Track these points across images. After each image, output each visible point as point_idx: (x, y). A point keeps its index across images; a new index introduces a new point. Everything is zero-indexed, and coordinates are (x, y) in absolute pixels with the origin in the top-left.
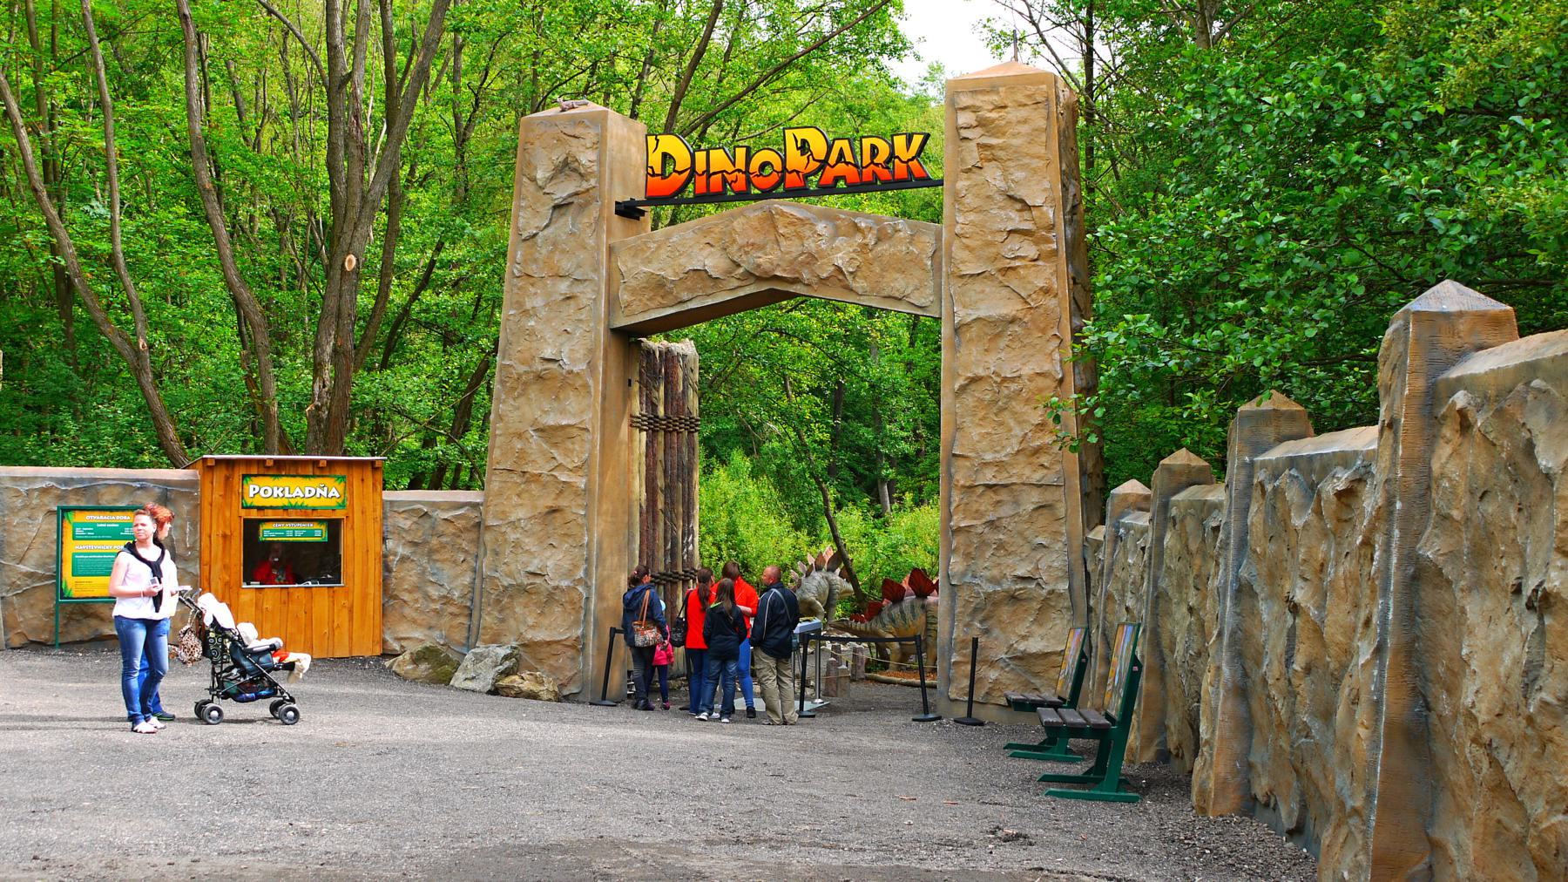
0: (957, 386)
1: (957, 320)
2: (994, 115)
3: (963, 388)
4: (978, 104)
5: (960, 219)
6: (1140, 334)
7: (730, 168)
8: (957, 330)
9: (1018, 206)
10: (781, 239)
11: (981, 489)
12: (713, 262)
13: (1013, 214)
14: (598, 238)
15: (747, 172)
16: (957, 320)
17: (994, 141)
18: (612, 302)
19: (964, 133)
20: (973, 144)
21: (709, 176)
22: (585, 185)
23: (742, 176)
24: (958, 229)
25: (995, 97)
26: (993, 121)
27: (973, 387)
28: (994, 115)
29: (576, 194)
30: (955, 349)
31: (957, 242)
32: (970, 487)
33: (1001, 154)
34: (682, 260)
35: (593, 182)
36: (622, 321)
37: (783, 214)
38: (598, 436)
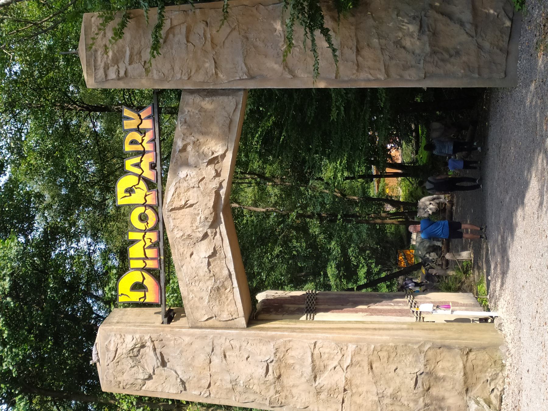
0: (290, 76)
1: (245, 77)
2: (110, 54)
3: (291, 72)
4: (102, 65)
5: (179, 76)
6: (59, 169)
7: (142, 243)
8: (252, 78)
9: (171, 36)
10: (190, 203)
11: (360, 59)
12: (204, 250)
13: (176, 39)
14: (185, 334)
15: (145, 231)
16: (245, 77)
17: (128, 53)
18: (228, 325)
19: (122, 74)
20: (129, 68)
21: (147, 258)
22: (149, 344)
23: (148, 235)
24: (185, 78)
25: (99, 53)
26: (114, 54)
27: (290, 65)
28: (110, 54)
29: (155, 350)
30: (264, 78)
31: (194, 79)
32: (358, 66)
33: (136, 50)
34: (201, 273)
35: (147, 338)
36: (242, 321)
37: (172, 201)
38: (320, 335)
